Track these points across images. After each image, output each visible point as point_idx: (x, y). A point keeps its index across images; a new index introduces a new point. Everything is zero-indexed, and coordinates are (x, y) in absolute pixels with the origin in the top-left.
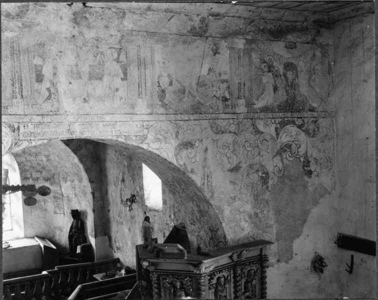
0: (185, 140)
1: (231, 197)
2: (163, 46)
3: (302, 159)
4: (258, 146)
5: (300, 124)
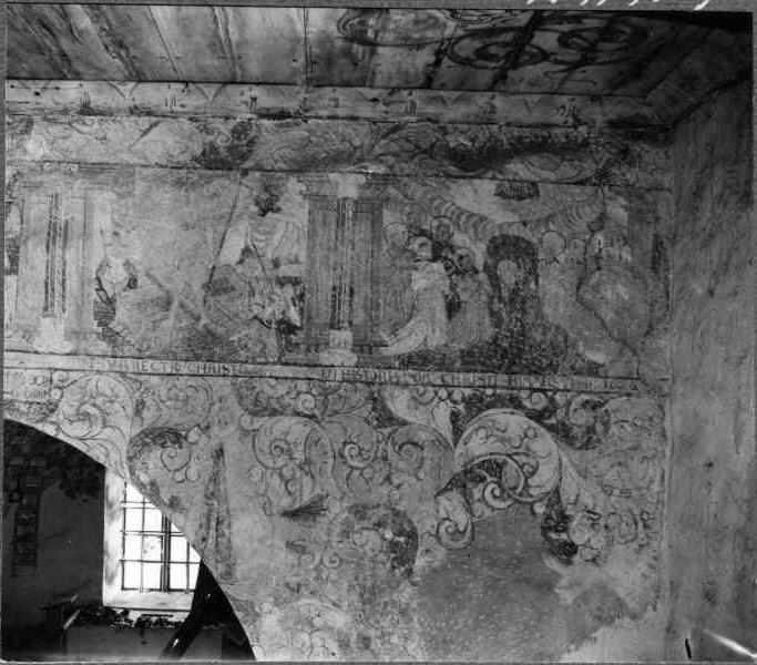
1: (287, 585)
2: (119, 195)
3: (540, 509)
4: (385, 458)
5: (539, 407)
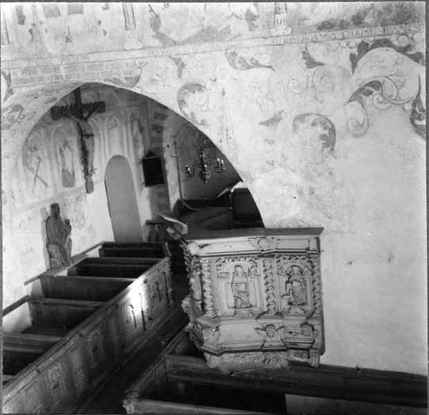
0: (191, 81)
1: (267, 162)
4: (313, 87)
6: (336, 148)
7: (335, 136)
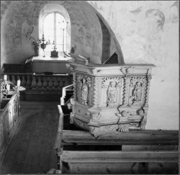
6: (164, 27)
7: (164, 21)
